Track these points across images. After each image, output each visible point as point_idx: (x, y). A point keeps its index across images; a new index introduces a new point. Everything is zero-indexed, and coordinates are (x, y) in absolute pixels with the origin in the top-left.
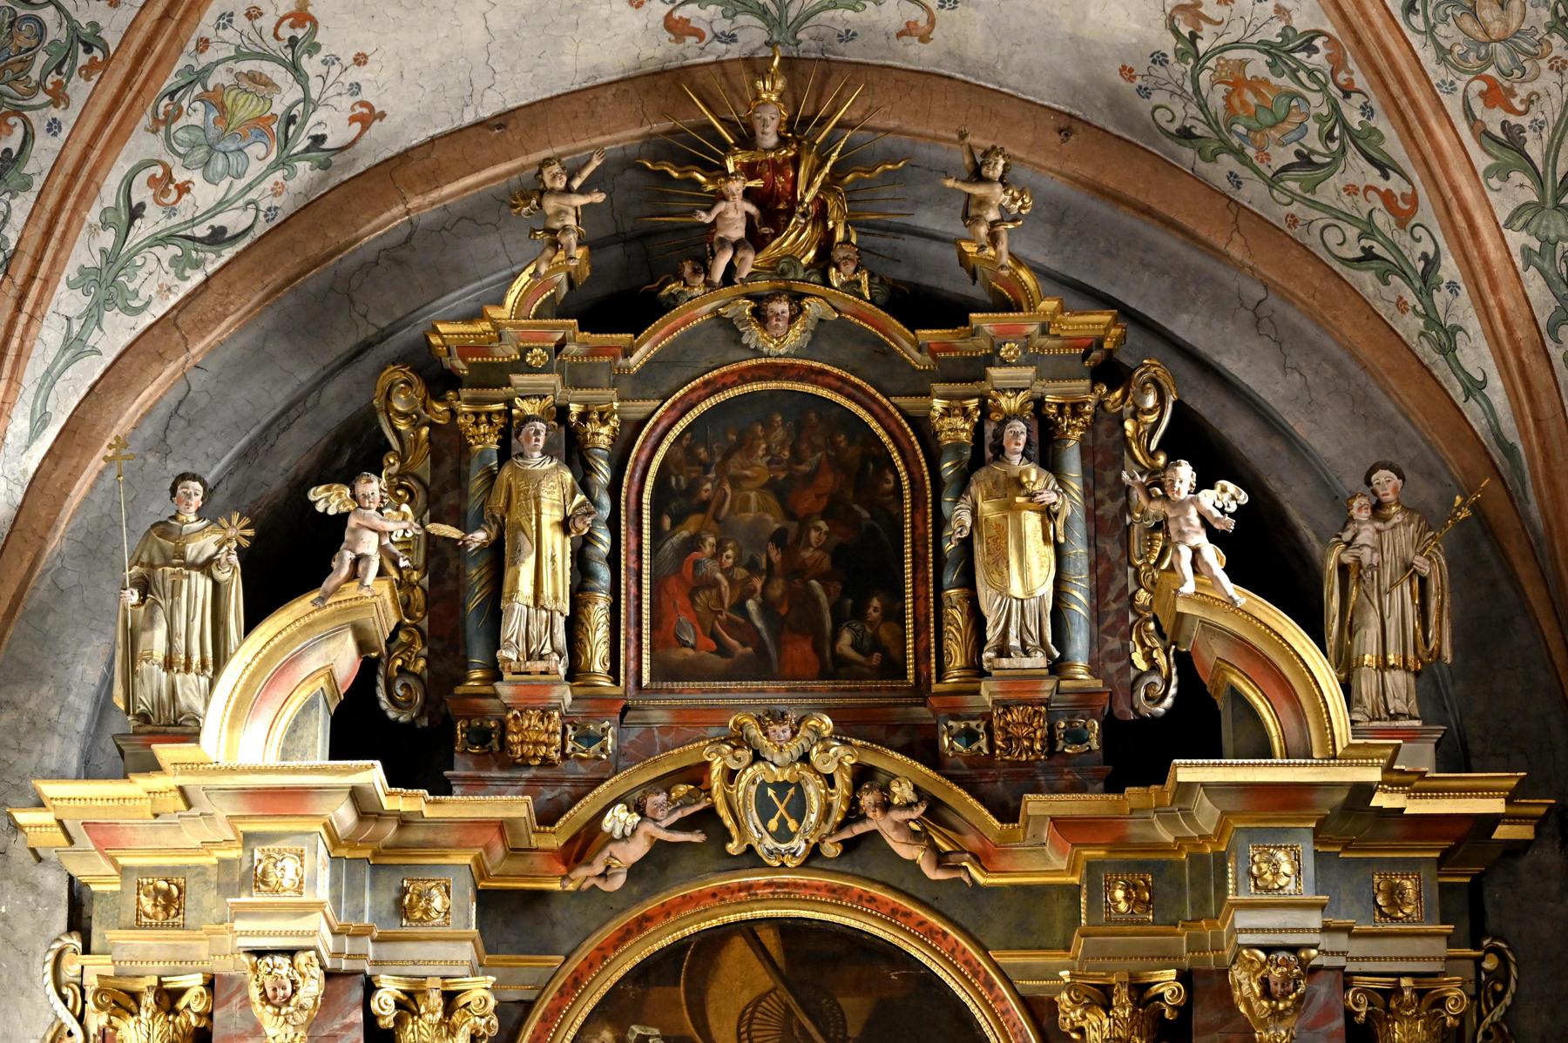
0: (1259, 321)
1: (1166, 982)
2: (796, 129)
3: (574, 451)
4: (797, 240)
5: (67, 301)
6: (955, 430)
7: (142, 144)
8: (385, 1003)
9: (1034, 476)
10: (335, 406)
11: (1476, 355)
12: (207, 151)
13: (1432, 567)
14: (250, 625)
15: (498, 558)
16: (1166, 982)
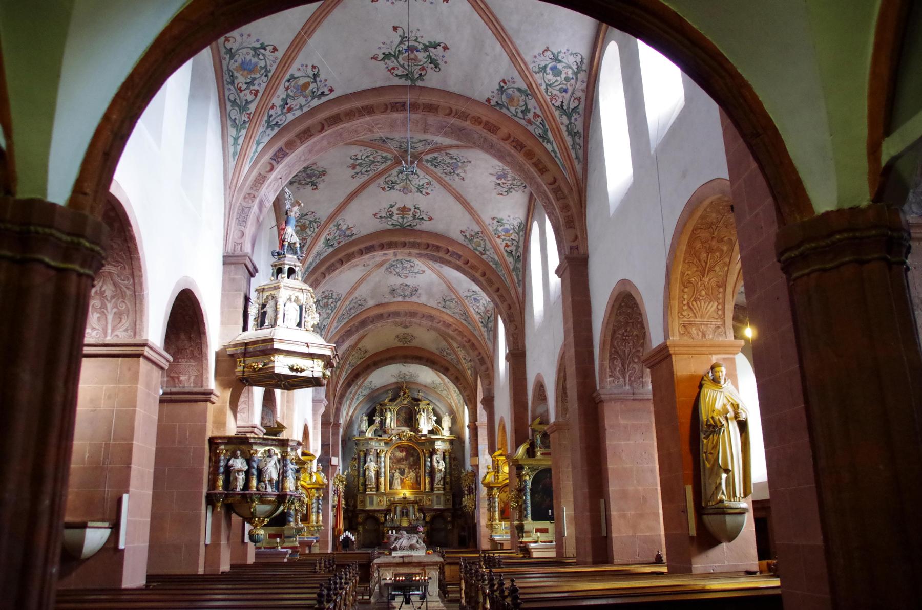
0: (439, 400)
1: (431, 450)
2: (406, 387)
3: (390, 411)
4: (406, 395)
5: (355, 400)
6: (418, 410)
7: (360, 390)
8: (378, 451)
9: (423, 414)
10: (373, 406)
11: (453, 404)
12: (364, 390)
13: (450, 420)
14: (368, 427)
15: (385, 419)
16: (431, 450)
